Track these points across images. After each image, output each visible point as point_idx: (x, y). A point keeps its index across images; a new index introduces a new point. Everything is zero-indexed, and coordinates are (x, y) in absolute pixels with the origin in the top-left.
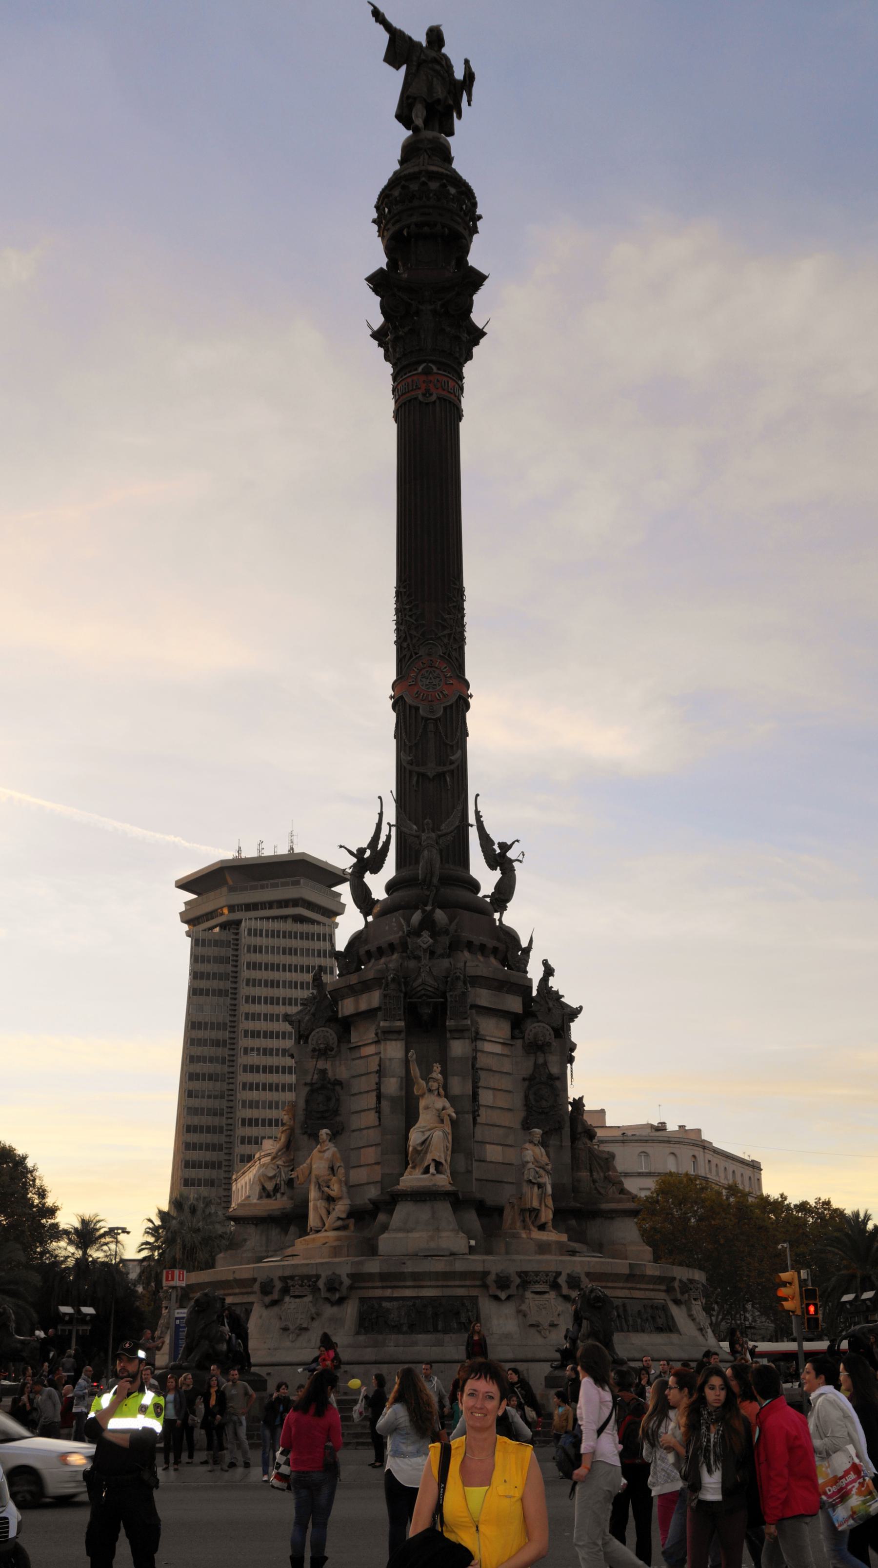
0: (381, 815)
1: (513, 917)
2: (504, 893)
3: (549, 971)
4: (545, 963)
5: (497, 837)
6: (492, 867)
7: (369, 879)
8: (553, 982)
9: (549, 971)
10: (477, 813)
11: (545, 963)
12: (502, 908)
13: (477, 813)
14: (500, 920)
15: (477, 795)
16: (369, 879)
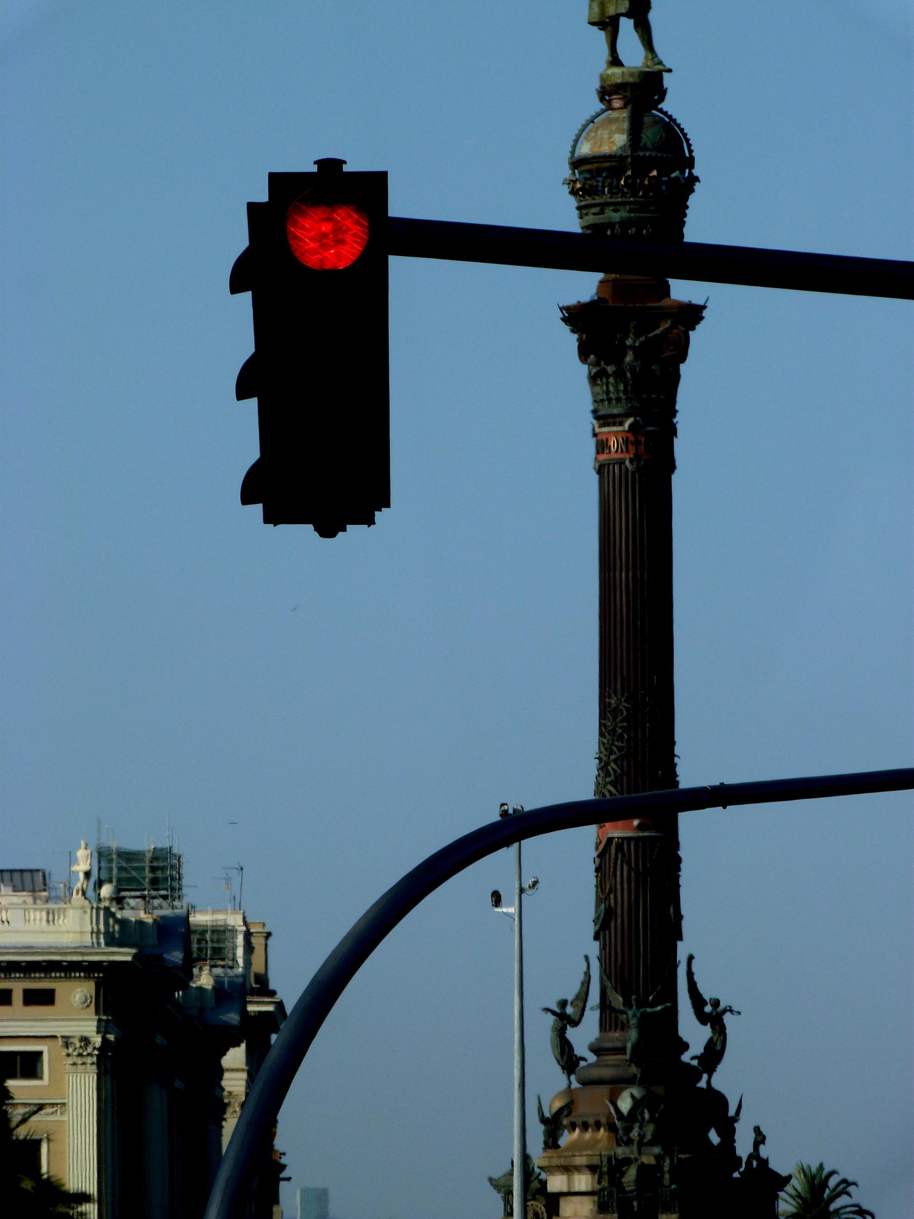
0: (588, 975)
1: (723, 1080)
2: (713, 1055)
3: (760, 1138)
4: (757, 1130)
5: (707, 993)
6: (704, 1023)
7: (571, 1033)
8: (764, 1151)
9: (760, 1138)
10: (690, 974)
11: (757, 1130)
12: (711, 1071)
13: (690, 974)
14: (709, 1082)
15: (691, 958)
16: (571, 1033)
